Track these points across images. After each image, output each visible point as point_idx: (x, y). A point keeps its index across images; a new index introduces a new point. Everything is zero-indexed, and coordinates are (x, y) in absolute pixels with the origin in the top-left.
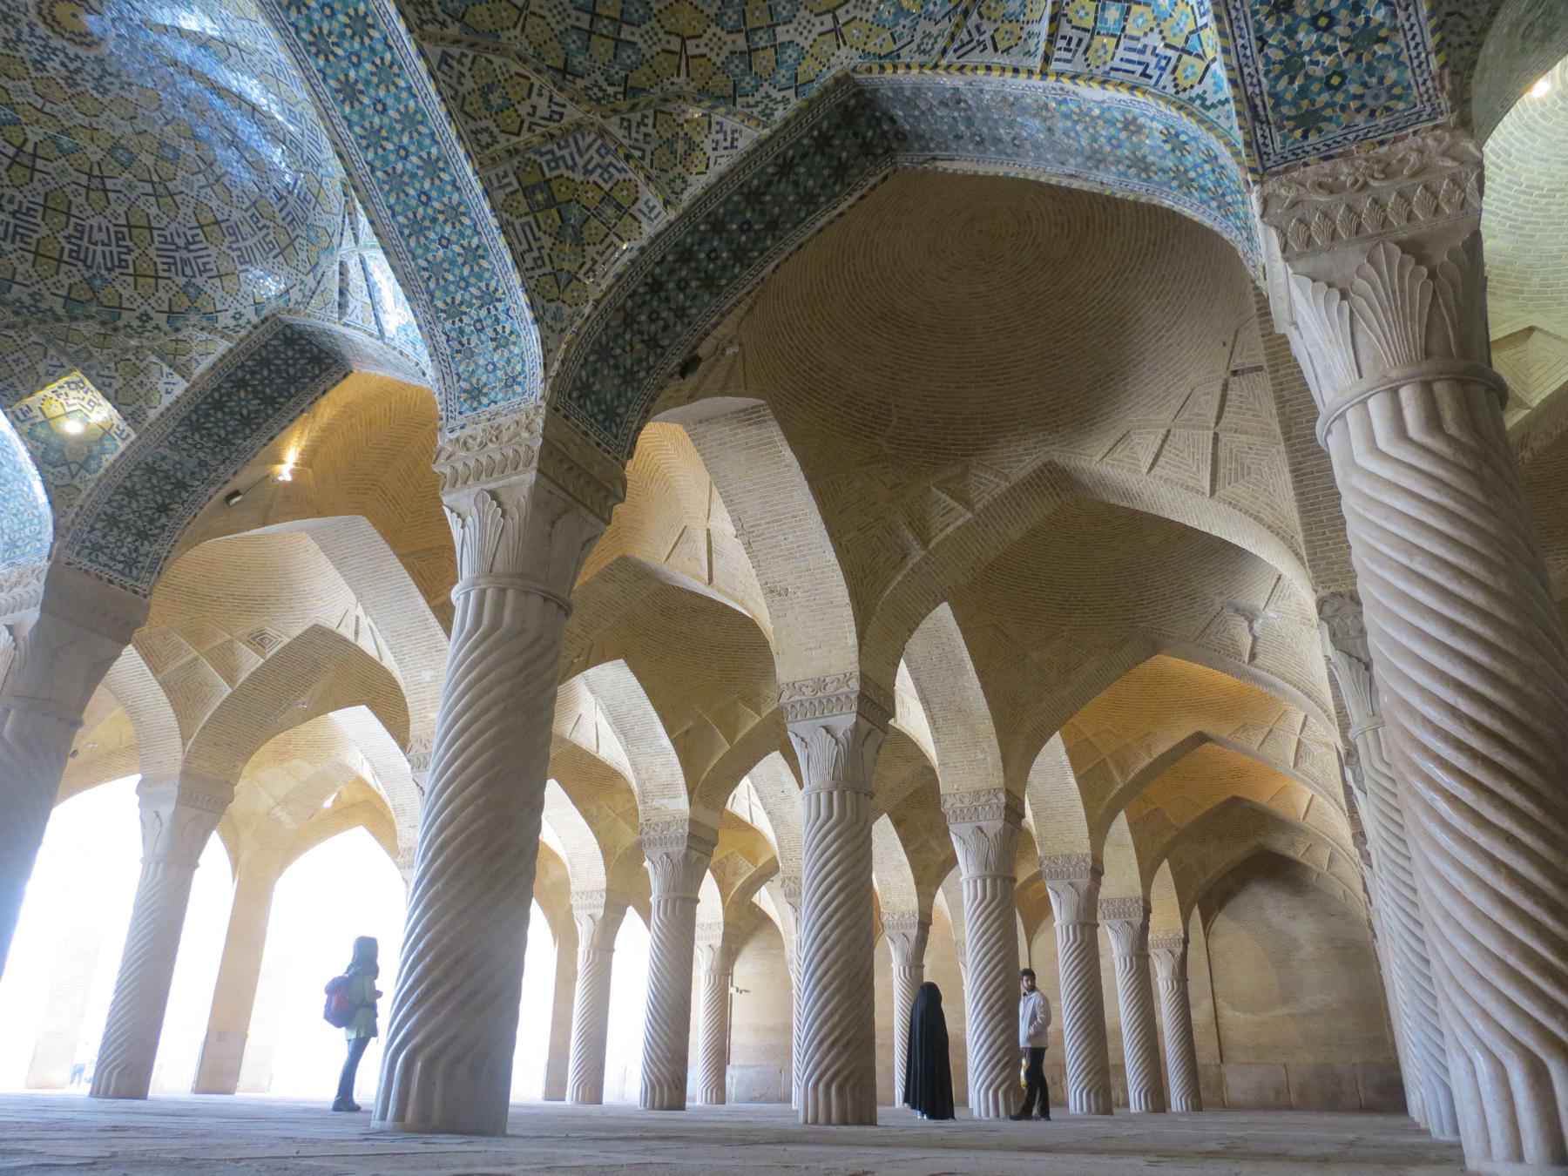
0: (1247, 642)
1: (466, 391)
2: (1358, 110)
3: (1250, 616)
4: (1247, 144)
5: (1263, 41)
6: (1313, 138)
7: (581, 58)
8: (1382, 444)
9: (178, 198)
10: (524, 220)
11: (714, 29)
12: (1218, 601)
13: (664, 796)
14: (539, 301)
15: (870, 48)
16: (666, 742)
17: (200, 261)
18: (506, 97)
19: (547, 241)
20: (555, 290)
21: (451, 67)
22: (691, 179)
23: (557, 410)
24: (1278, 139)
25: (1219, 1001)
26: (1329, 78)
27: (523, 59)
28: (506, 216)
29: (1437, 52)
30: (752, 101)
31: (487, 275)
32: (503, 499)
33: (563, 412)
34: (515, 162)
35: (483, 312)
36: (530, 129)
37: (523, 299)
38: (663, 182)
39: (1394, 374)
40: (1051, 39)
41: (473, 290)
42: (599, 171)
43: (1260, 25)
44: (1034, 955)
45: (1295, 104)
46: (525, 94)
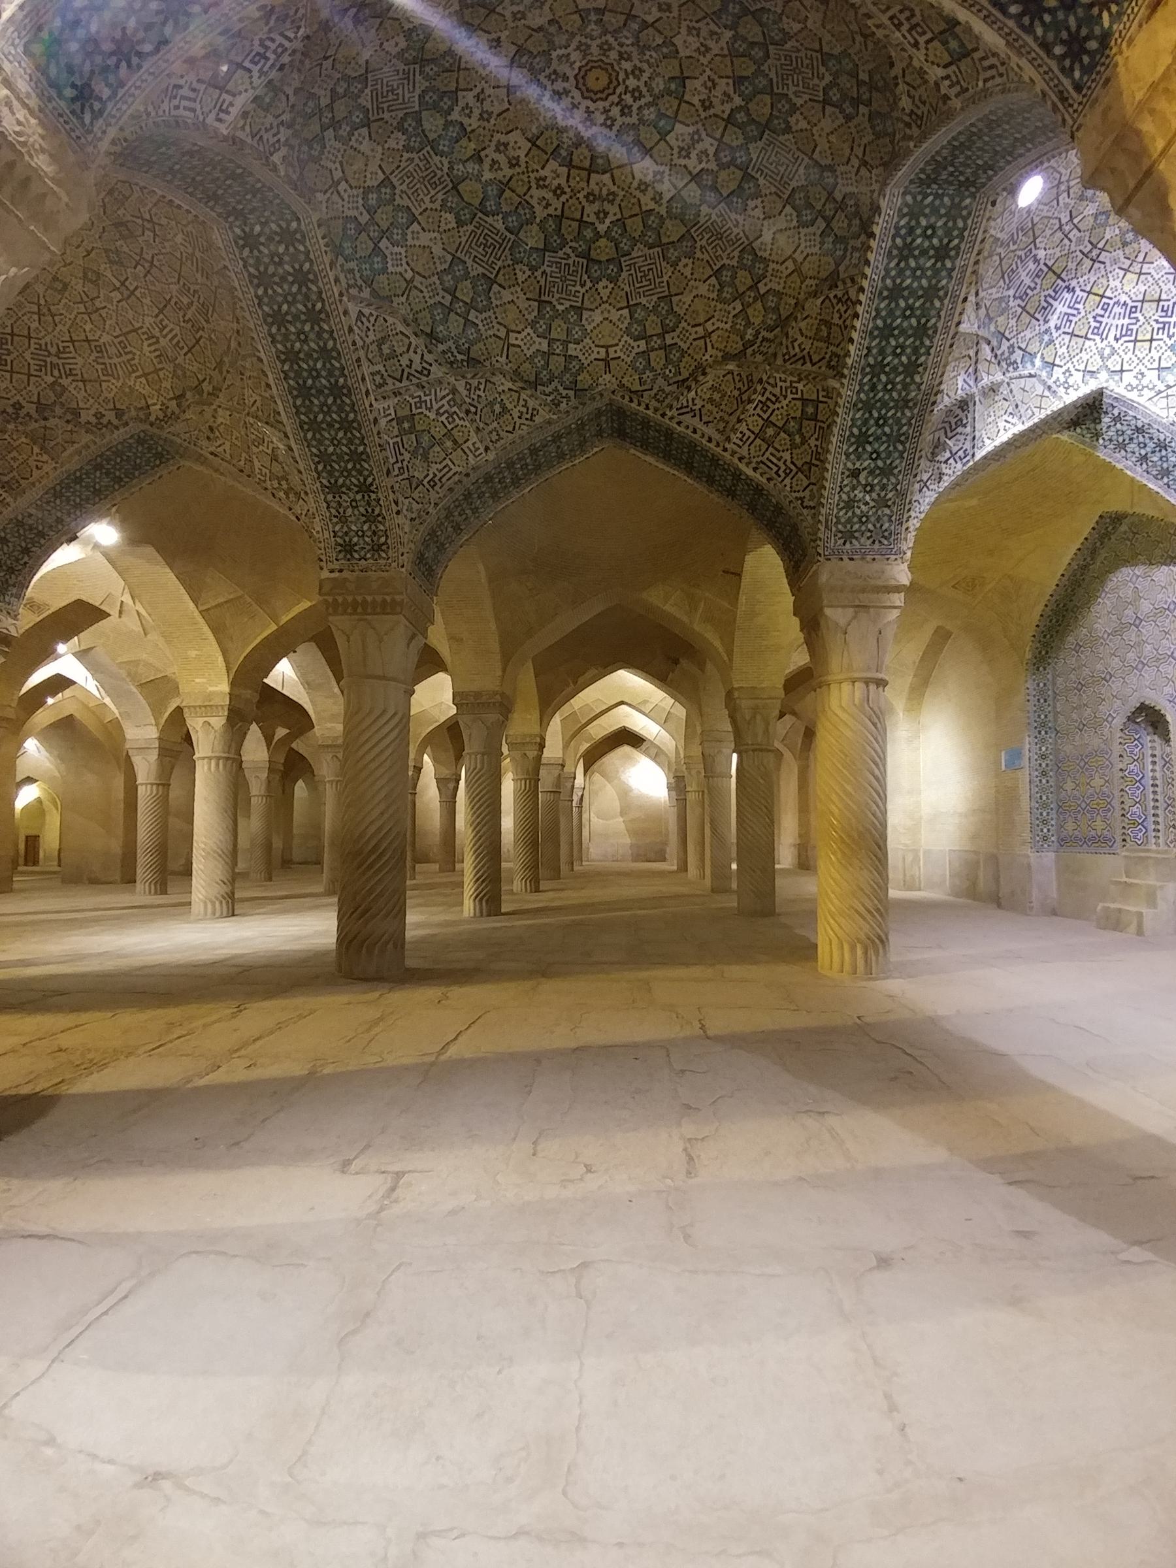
1: (341, 545)
2: (868, 538)
6: (848, 545)
7: (441, 328)
9: (57, 319)
10: (395, 440)
11: (529, 330)
15: (624, 381)
17: (67, 367)
19: (407, 456)
27: (406, 322)
35: (359, 497)
42: (446, 415)
46: (405, 349)
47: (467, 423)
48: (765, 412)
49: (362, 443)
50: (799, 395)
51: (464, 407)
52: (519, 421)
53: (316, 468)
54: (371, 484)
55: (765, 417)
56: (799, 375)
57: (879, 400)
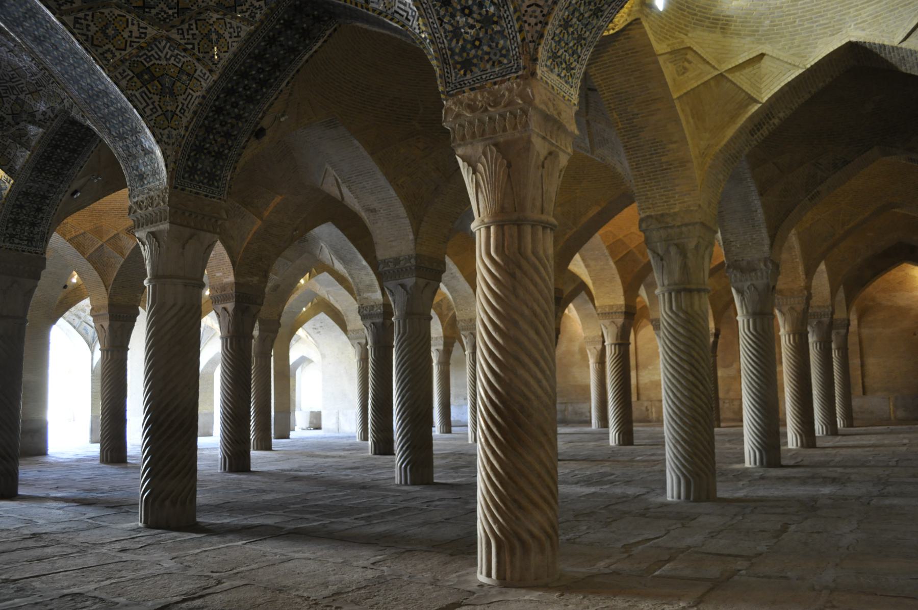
2: (488, 61)
5: (441, 20)
6: (469, 76)
10: (140, 90)
13: (369, 292)
14: (157, 131)
16: (364, 263)
18: (116, 29)
19: (156, 98)
20: (166, 122)
21: (81, 24)
23: (176, 188)
24: (454, 74)
26: (474, 41)
30: (244, 8)
33: (180, 187)
34: (127, 64)
36: (131, 46)
38: (206, 60)
44: (638, 340)
47: (189, 59)
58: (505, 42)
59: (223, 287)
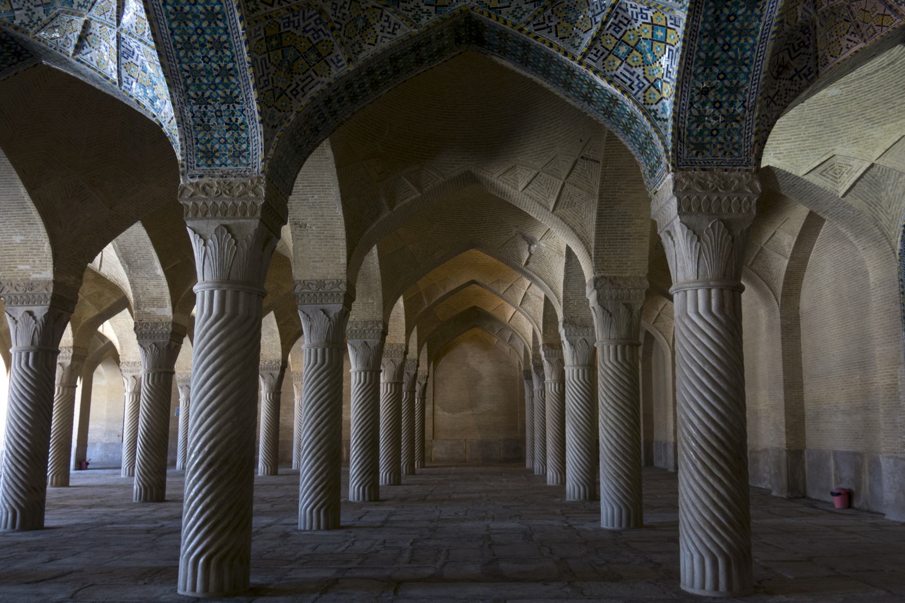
0: (526, 255)
1: (201, 151)
2: (720, 150)
3: (531, 242)
4: (673, 151)
5: (691, 104)
6: (700, 157)
8: (701, 310)
10: (263, 56)
12: (515, 230)
16: (160, 271)
22: (365, 46)
25: (436, 406)
28: (255, 55)
29: (756, 134)
31: (233, 86)
32: (235, 232)
35: (224, 107)
37: (256, 108)
39: (712, 283)
40: (590, 48)
41: (220, 92)
42: (312, 32)
43: (693, 97)
45: (696, 138)
47: (331, 38)
48: (617, 32)
49: (232, 60)
50: (649, 20)
51: (330, 25)
52: (380, 35)
53: (185, 82)
54: (237, 97)
55: (618, 37)
56: (648, 4)
57: (723, 29)
58: (740, 138)
59: (31, 285)
